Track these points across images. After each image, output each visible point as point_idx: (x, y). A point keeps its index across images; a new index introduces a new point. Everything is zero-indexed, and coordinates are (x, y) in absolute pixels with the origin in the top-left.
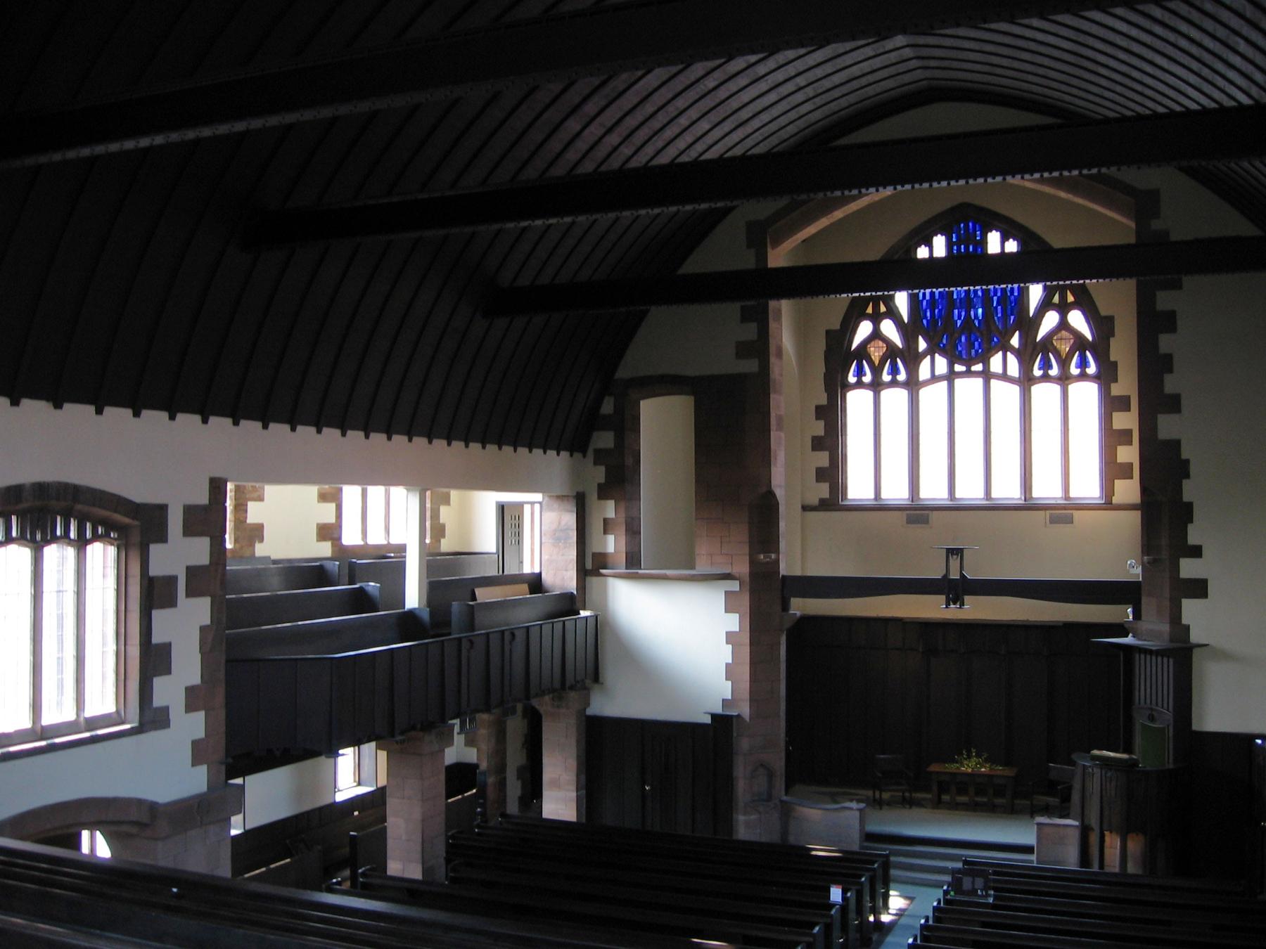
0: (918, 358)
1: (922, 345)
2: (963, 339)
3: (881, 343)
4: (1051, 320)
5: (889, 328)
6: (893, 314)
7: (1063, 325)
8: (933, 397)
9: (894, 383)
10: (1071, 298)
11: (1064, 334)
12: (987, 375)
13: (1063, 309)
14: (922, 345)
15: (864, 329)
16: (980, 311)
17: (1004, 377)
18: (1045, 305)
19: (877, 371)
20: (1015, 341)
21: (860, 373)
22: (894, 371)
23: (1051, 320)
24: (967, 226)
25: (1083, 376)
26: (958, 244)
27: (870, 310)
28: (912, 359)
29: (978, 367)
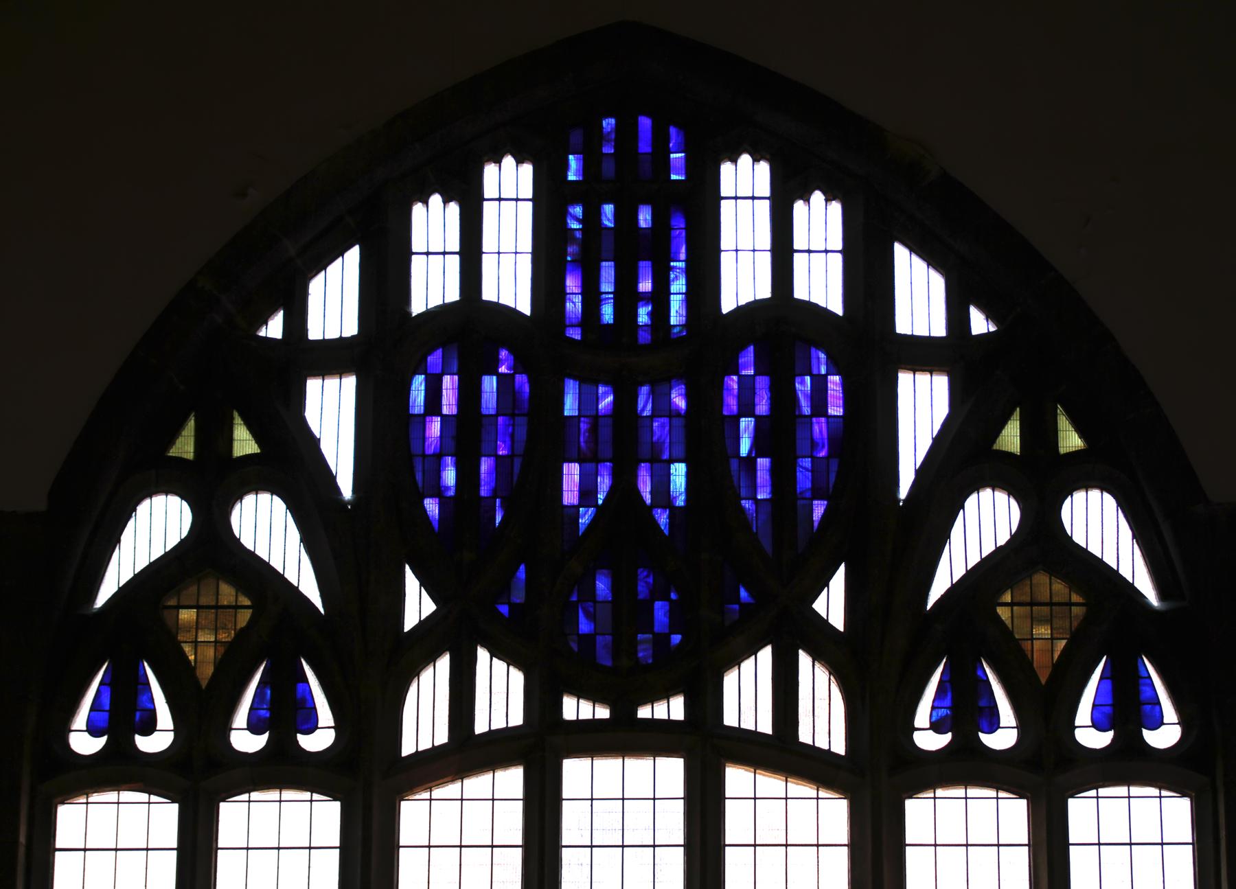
1: (417, 605)
2: (602, 586)
3: (227, 593)
4: (987, 521)
5: (265, 526)
6: (289, 464)
7: (1041, 541)
9: (282, 769)
10: (1070, 440)
11: (1049, 586)
12: (708, 751)
14: (417, 605)
15: (157, 527)
16: (679, 471)
17: (782, 752)
18: (960, 462)
20: (832, 604)
21: (122, 718)
22: (283, 715)
23: (987, 521)
24: (626, 133)
25: (1128, 764)
26: (588, 193)
27: (185, 446)
28: (372, 672)
29: (674, 709)
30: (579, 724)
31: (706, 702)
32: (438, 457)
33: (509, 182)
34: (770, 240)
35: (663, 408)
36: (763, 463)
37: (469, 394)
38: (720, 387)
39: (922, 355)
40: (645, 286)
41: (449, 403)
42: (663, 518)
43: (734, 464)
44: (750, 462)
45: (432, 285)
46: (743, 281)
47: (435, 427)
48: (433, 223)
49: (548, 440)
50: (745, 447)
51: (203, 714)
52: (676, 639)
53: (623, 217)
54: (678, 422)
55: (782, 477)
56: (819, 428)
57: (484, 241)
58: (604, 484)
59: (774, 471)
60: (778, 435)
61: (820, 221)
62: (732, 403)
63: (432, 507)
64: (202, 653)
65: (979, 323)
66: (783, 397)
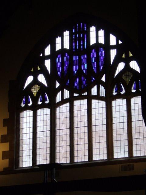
0: (56, 91)
1: (58, 85)
2: (78, 80)
3: (37, 86)
4: (121, 66)
5: (41, 78)
6: (44, 71)
7: (127, 68)
8: (63, 111)
10: (131, 55)
11: (128, 73)
12: (90, 98)
13: (127, 61)
14: (58, 85)
15: (30, 79)
16: (86, 65)
17: (98, 97)
18: (118, 59)
19: (35, 100)
20: (103, 79)
21: (27, 102)
22: (44, 100)
23: (121, 66)
29: (86, 94)
30: (76, 96)
31: (89, 92)
32: (59, 67)
33: (66, 34)
34: (96, 36)
35: (84, 58)
36: (95, 63)
37: (63, 59)
38: (91, 55)
39: (113, 47)
40: (82, 44)
41: (60, 61)
42: (84, 71)
43: (92, 63)
44: (94, 63)
45: (58, 47)
46: (93, 41)
47: (59, 64)
48: (58, 40)
49: (71, 63)
50: (93, 61)
51: (35, 100)
52: (86, 85)
53: (79, 37)
54: (86, 59)
55: (98, 64)
56: (102, 58)
57: (64, 41)
58: (78, 68)
59: (96, 64)
60: (97, 59)
61: (101, 33)
62: (92, 56)
63: (59, 73)
64: (35, 94)
65: (120, 42)
66: (98, 55)
